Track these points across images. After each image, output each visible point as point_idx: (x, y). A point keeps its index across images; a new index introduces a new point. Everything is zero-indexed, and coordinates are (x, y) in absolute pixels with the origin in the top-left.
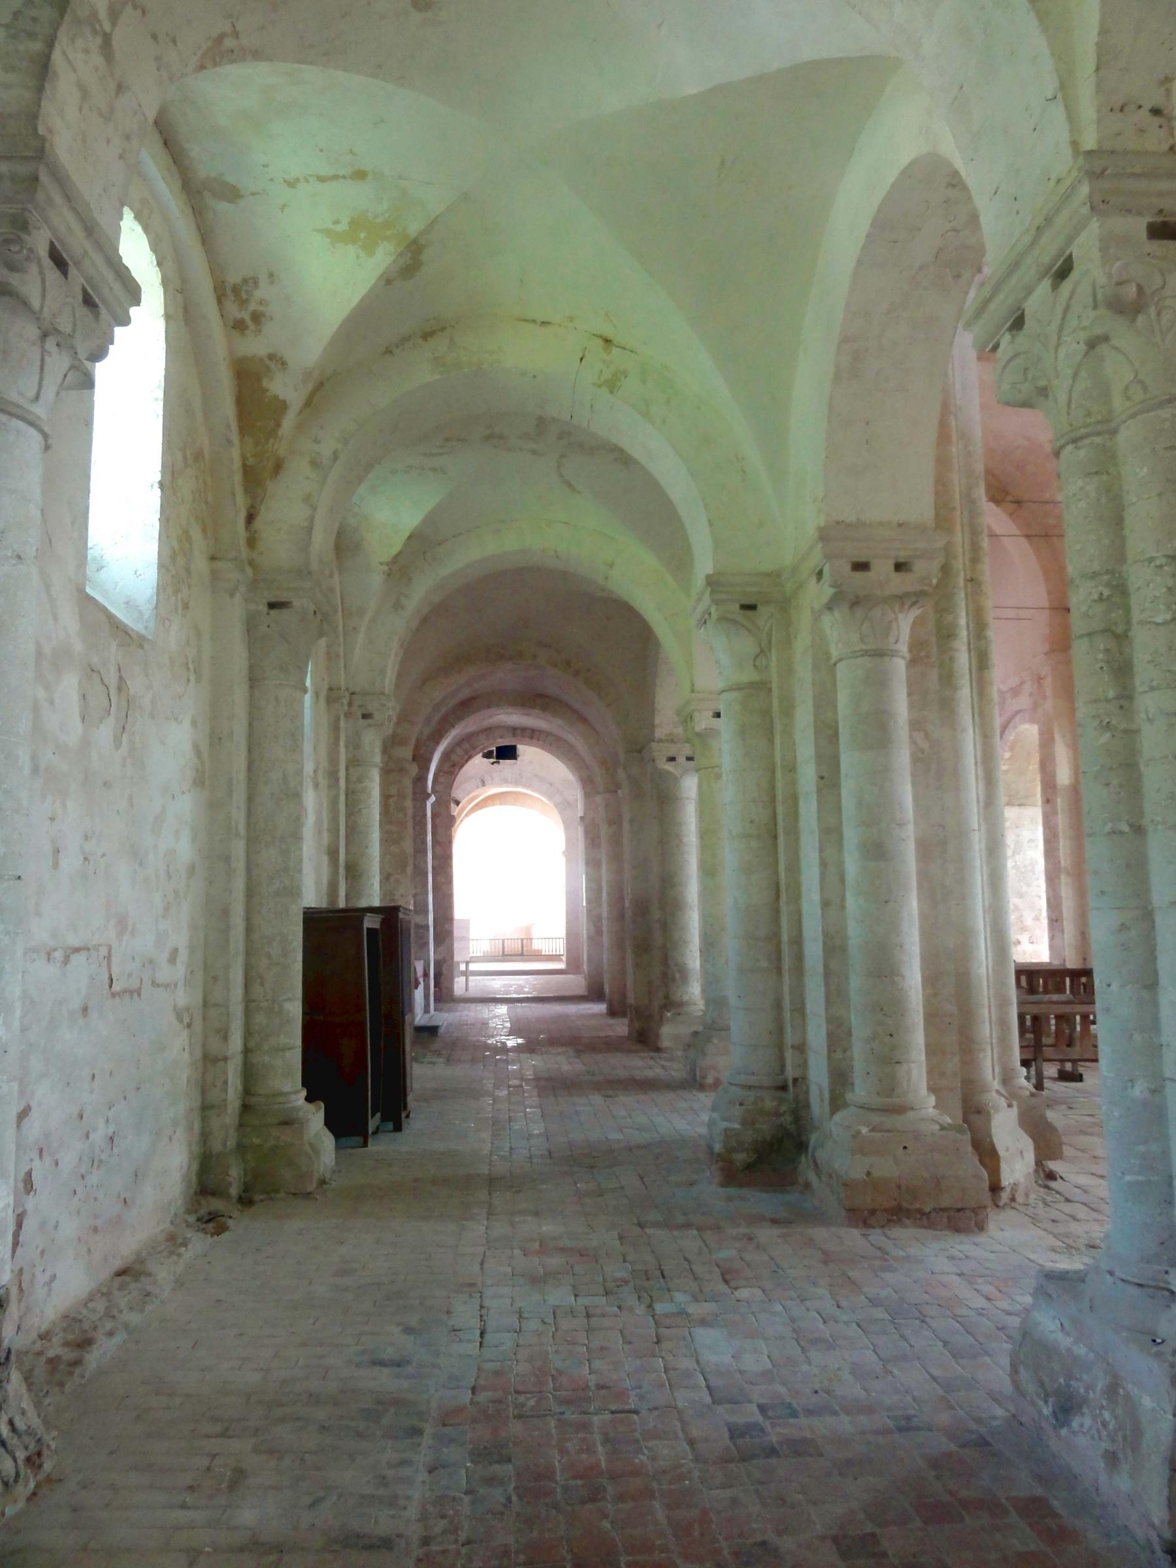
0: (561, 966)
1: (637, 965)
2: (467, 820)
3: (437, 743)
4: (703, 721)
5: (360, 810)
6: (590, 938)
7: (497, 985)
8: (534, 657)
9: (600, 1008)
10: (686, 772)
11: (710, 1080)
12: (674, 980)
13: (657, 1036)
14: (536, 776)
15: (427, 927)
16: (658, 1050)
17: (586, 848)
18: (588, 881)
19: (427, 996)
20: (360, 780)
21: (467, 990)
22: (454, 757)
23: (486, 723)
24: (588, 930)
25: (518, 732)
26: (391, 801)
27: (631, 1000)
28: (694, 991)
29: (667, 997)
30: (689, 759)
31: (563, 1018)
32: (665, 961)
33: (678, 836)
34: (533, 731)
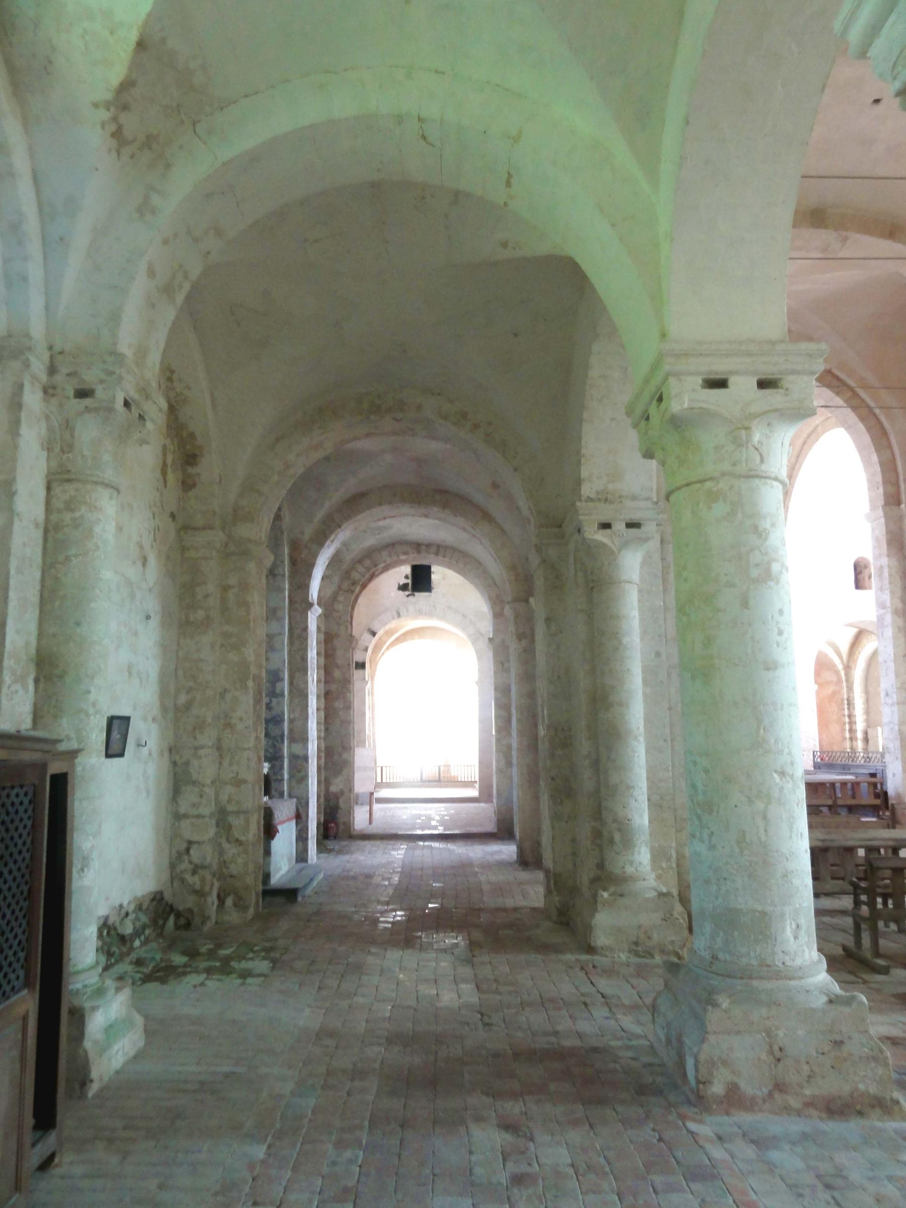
0: (474, 793)
1: (556, 817)
2: (388, 653)
3: (321, 545)
4: (687, 395)
5: (67, 559)
6: (500, 771)
7: (405, 816)
8: (419, 407)
10: (625, 544)
11: (717, 1088)
12: (611, 841)
13: (588, 929)
14: (449, 607)
15: (306, 758)
16: (591, 950)
17: (495, 673)
19: (302, 837)
20: (70, 506)
21: (370, 823)
22: (355, 575)
23: (385, 537)
24: (497, 761)
25: (423, 547)
26: (231, 594)
27: (548, 859)
28: (641, 861)
29: (601, 866)
30: (631, 525)
31: (463, 867)
32: (598, 813)
33: (616, 636)
34: (439, 546)
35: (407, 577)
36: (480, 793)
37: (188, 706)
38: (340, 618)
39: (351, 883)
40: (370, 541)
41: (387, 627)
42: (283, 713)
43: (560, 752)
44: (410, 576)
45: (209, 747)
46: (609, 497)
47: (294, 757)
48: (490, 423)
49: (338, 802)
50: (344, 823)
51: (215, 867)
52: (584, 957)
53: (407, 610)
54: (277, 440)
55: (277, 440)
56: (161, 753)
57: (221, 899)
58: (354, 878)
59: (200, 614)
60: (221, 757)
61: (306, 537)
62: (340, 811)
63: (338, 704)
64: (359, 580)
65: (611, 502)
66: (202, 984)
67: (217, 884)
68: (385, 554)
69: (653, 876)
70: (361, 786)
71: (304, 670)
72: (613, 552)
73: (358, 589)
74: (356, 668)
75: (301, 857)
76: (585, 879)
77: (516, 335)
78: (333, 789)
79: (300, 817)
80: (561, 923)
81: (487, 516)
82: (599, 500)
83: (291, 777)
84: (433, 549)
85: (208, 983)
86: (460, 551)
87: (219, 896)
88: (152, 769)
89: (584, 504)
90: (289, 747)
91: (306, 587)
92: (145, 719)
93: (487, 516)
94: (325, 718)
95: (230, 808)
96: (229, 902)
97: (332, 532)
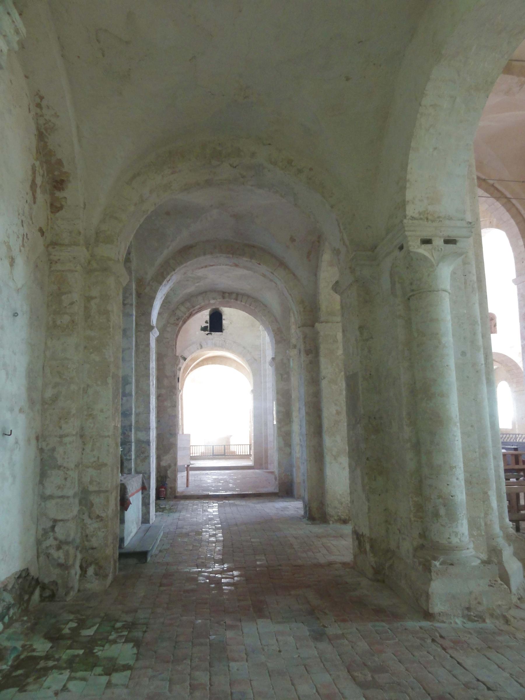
3: (160, 283)
6: (280, 449)
7: (209, 480)
8: (253, 155)
9: (293, 507)
10: (443, 258)
12: (436, 515)
14: (235, 342)
15: (148, 443)
16: (428, 616)
17: (277, 382)
18: (278, 404)
19: (146, 504)
21: (187, 486)
22: (178, 313)
26: (93, 304)
29: (423, 535)
30: (447, 242)
31: (266, 523)
34: (238, 294)
35: (206, 322)
36: (255, 462)
37: (55, 399)
39: (186, 540)
40: (191, 289)
41: (194, 355)
42: (132, 410)
43: (373, 437)
45: (74, 435)
46: (430, 217)
47: (139, 442)
48: (311, 169)
50: (171, 488)
51: (78, 541)
52: (425, 624)
53: (207, 344)
54: (134, 177)
55: (134, 177)
56: (29, 441)
57: (83, 569)
58: (187, 535)
59: (66, 319)
60: (84, 444)
61: (149, 277)
62: (168, 479)
63: (167, 404)
64: (182, 317)
65: (433, 221)
66: (65, 688)
67: (79, 556)
68: (200, 298)
69: (471, 546)
70: (181, 462)
71: (147, 376)
72: (432, 266)
73: (181, 323)
75: (145, 519)
76: (406, 547)
77: (348, 79)
78: (163, 464)
79: (145, 488)
80: (378, 581)
81: (282, 264)
82: (421, 219)
83: (137, 456)
84: (234, 296)
85: (71, 685)
86: (253, 298)
87: (81, 567)
88: (18, 456)
89: (410, 221)
90: (135, 433)
91: (149, 314)
92: (12, 410)
93: (282, 264)
95: (91, 488)
96: (91, 571)
97: (168, 274)
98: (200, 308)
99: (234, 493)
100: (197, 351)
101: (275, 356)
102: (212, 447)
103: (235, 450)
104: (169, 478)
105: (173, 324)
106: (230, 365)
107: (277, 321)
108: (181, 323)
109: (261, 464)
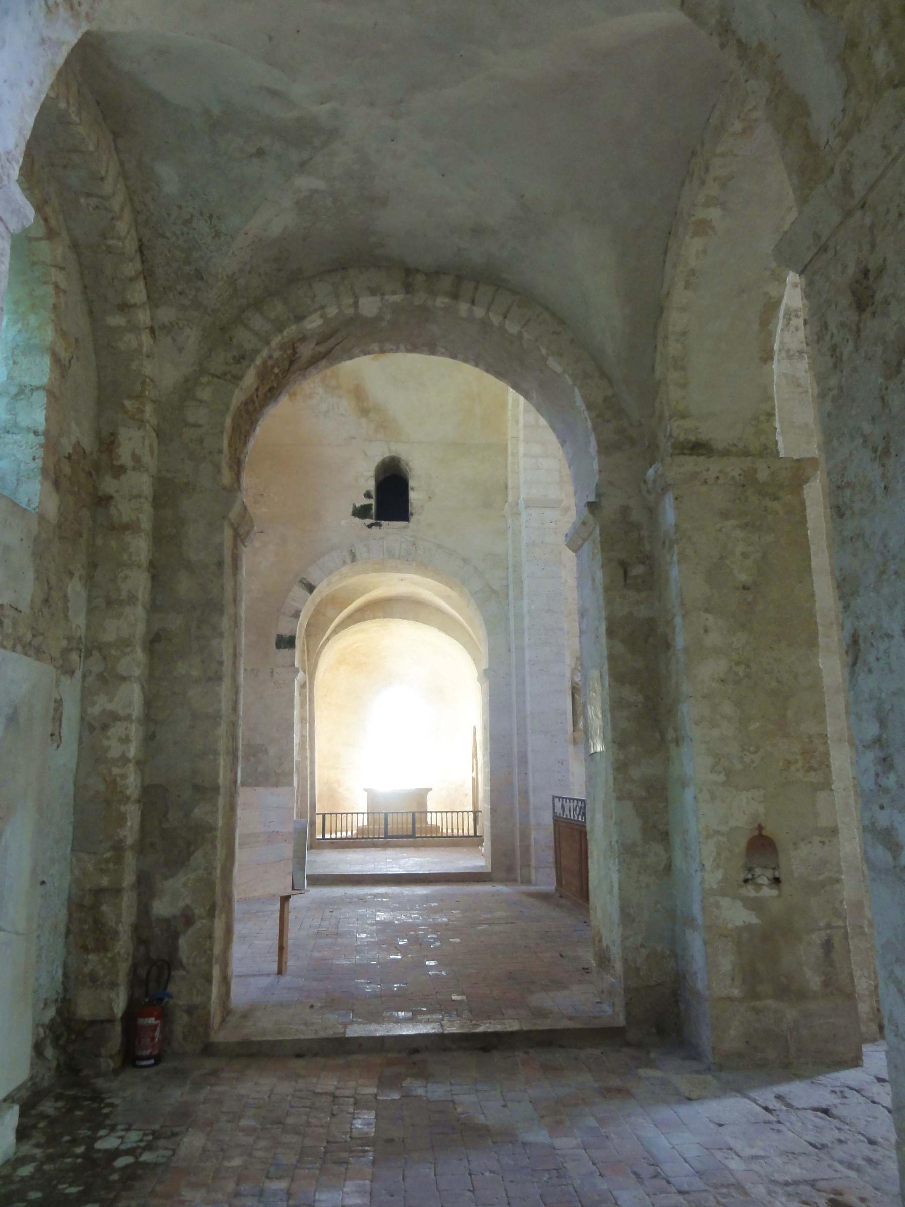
0: (477, 860)
14: (440, 546)
21: (280, 972)
22: (242, 336)
35: (368, 495)
36: (493, 864)
38: (201, 441)
44: (373, 494)
49: (175, 948)
50: (190, 1010)
62: (178, 973)
64: (257, 351)
68: (322, 289)
74: (278, 646)
78: (162, 908)
84: (446, 282)
94: (148, 704)
98: (323, 338)
99: (452, 1028)
100: (345, 570)
101: (599, 495)
102: (382, 816)
103: (439, 824)
104: (181, 965)
105: (222, 376)
106: (426, 621)
107: (604, 375)
108: (250, 378)
109: (510, 869)
